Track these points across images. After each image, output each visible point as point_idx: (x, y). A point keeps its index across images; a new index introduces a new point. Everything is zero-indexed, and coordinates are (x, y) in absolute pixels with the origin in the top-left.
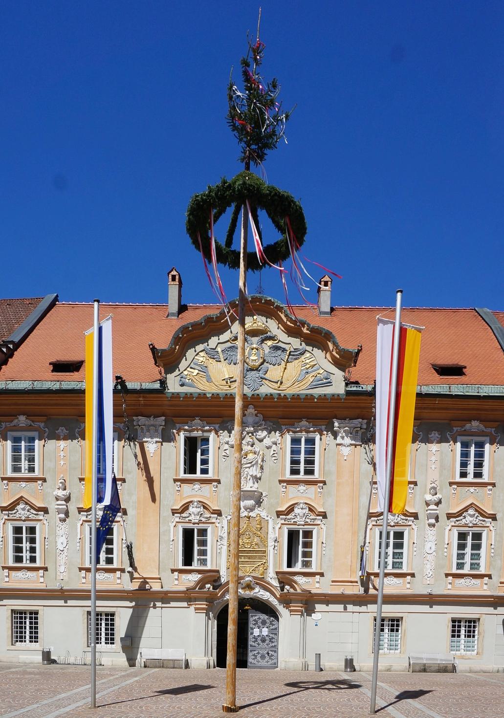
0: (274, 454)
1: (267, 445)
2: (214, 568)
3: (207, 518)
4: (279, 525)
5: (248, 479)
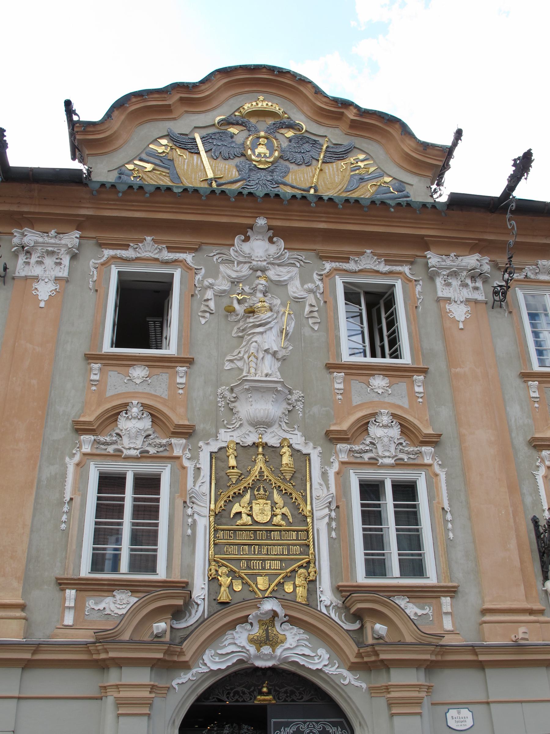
0: (311, 312)
1: (296, 295)
2: (176, 577)
3: (161, 446)
4: (336, 467)
5: (260, 358)
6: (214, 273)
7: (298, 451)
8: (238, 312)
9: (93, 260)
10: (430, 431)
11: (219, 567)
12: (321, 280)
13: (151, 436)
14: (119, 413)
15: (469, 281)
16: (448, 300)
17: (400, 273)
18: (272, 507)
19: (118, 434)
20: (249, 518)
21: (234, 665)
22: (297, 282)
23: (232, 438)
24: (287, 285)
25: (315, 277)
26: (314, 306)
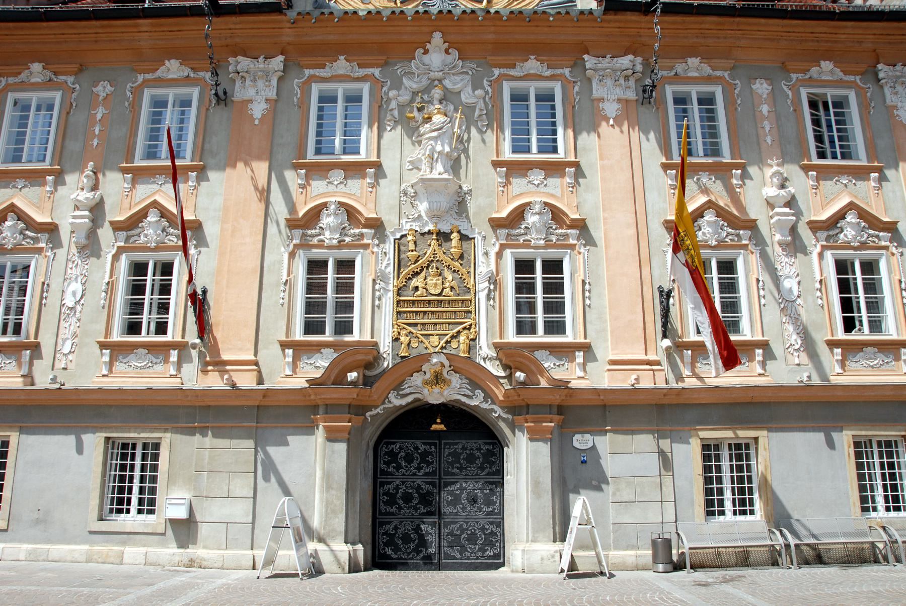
0: (480, 115)
1: (468, 101)
6: (397, 85)
7: (466, 236)
8: (417, 119)
9: (296, 80)
10: (577, 216)
11: (401, 329)
12: (490, 86)
13: (347, 228)
14: (321, 211)
15: (622, 81)
16: (602, 100)
17: (561, 75)
18: (443, 282)
19: (321, 228)
20: (425, 290)
21: (412, 402)
22: (469, 89)
23: (412, 227)
24: (460, 92)
25: (485, 82)
26: (483, 110)
